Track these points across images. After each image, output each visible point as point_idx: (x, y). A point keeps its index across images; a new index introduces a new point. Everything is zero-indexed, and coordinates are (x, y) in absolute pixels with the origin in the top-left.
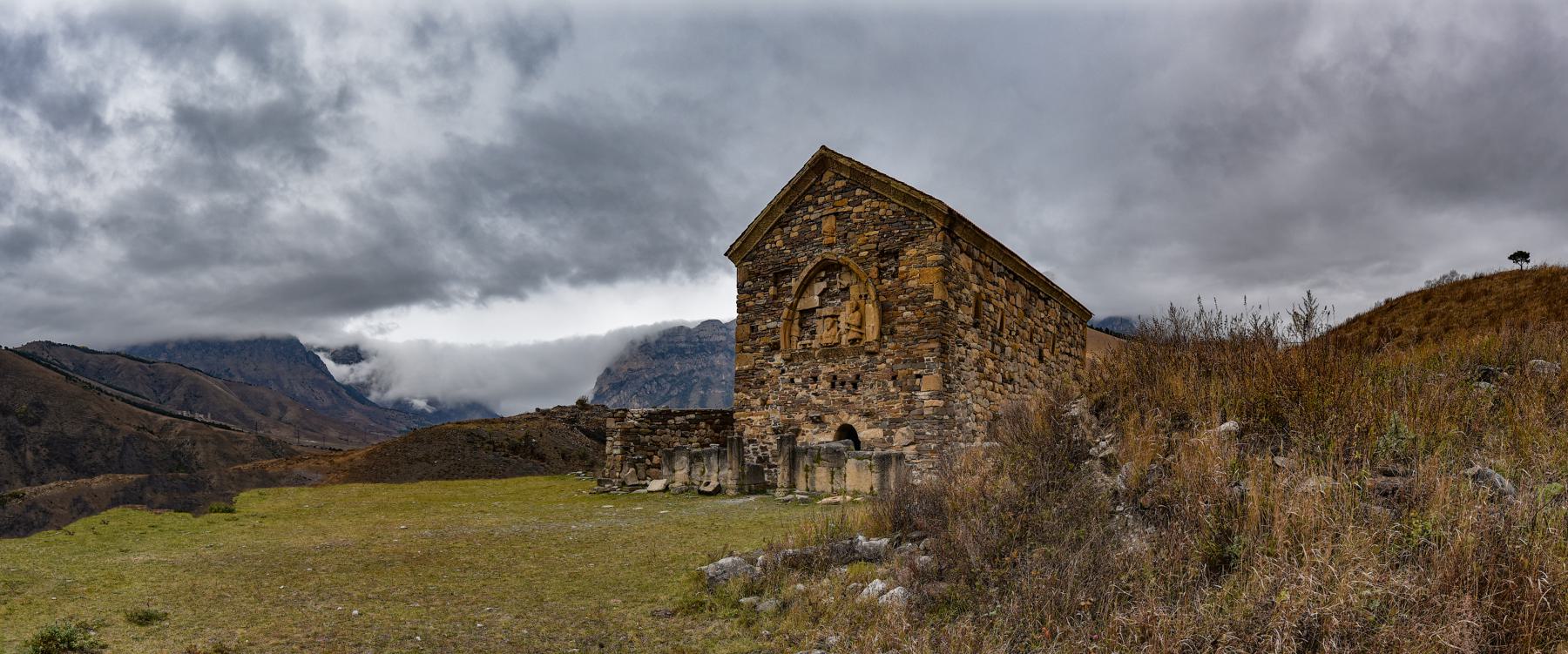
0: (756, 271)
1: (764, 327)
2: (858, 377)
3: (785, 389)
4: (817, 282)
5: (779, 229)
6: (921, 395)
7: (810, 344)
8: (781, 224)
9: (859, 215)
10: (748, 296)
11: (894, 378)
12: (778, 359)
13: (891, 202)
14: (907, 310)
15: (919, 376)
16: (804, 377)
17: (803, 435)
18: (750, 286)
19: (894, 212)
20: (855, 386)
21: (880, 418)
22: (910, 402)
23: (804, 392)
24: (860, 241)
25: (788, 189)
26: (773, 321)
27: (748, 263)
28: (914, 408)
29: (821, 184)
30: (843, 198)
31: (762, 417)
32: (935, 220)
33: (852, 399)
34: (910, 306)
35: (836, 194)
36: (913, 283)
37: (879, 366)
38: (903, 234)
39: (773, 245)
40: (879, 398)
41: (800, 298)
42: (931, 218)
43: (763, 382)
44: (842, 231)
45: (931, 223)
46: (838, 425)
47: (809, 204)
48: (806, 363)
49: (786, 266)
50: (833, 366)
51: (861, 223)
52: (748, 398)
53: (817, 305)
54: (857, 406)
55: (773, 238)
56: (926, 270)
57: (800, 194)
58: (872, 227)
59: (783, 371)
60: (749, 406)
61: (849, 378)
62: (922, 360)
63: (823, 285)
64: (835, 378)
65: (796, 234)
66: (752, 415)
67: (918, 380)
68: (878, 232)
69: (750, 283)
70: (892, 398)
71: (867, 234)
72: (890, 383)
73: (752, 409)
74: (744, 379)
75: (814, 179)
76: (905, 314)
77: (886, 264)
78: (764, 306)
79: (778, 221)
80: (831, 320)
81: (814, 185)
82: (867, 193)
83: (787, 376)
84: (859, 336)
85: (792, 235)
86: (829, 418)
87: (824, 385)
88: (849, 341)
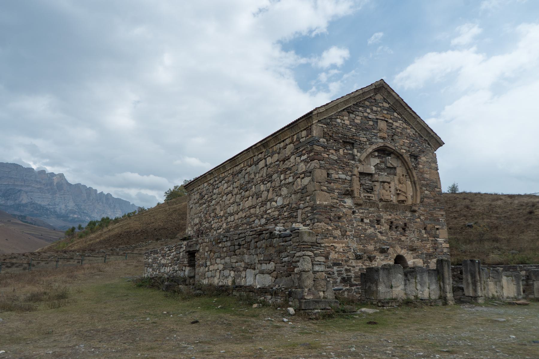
0: (330, 134)
1: (337, 176)
2: (405, 224)
3: (359, 226)
4: (372, 157)
5: (347, 113)
6: (440, 240)
7: (372, 197)
8: (349, 111)
10: (323, 149)
11: (425, 229)
12: (349, 202)
13: (412, 128)
14: (427, 190)
15: (437, 229)
16: (371, 219)
17: (375, 261)
18: (324, 142)
19: (413, 134)
21: (420, 252)
22: (435, 244)
23: (372, 230)
24: (401, 143)
25: (361, 92)
26: (343, 174)
27: (324, 126)
28: (438, 248)
29: (375, 99)
30: (387, 114)
31: (344, 245)
32: (433, 146)
33: (403, 238)
35: (384, 109)
38: (419, 148)
39: (343, 122)
40: (418, 239)
42: (431, 144)
43: (339, 218)
45: (430, 147)
46: (395, 255)
47: (368, 107)
50: (390, 215)
52: (330, 228)
53: (374, 172)
54: (406, 243)
55: (343, 116)
57: (364, 99)
58: (406, 138)
59: (354, 212)
60: (331, 235)
61: (401, 225)
62: (438, 220)
63: (377, 161)
64: (392, 222)
66: (335, 243)
67: (438, 231)
68: (408, 141)
70: (425, 241)
71: (404, 140)
72: (423, 231)
73: (335, 238)
74: (325, 213)
75: (372, 95)
76: (426, 192)
81: (370, 97)
82: (400, 117)
83: (358, 216)
85: (356, 121)
86: (391, 250)
87: (385, 227)
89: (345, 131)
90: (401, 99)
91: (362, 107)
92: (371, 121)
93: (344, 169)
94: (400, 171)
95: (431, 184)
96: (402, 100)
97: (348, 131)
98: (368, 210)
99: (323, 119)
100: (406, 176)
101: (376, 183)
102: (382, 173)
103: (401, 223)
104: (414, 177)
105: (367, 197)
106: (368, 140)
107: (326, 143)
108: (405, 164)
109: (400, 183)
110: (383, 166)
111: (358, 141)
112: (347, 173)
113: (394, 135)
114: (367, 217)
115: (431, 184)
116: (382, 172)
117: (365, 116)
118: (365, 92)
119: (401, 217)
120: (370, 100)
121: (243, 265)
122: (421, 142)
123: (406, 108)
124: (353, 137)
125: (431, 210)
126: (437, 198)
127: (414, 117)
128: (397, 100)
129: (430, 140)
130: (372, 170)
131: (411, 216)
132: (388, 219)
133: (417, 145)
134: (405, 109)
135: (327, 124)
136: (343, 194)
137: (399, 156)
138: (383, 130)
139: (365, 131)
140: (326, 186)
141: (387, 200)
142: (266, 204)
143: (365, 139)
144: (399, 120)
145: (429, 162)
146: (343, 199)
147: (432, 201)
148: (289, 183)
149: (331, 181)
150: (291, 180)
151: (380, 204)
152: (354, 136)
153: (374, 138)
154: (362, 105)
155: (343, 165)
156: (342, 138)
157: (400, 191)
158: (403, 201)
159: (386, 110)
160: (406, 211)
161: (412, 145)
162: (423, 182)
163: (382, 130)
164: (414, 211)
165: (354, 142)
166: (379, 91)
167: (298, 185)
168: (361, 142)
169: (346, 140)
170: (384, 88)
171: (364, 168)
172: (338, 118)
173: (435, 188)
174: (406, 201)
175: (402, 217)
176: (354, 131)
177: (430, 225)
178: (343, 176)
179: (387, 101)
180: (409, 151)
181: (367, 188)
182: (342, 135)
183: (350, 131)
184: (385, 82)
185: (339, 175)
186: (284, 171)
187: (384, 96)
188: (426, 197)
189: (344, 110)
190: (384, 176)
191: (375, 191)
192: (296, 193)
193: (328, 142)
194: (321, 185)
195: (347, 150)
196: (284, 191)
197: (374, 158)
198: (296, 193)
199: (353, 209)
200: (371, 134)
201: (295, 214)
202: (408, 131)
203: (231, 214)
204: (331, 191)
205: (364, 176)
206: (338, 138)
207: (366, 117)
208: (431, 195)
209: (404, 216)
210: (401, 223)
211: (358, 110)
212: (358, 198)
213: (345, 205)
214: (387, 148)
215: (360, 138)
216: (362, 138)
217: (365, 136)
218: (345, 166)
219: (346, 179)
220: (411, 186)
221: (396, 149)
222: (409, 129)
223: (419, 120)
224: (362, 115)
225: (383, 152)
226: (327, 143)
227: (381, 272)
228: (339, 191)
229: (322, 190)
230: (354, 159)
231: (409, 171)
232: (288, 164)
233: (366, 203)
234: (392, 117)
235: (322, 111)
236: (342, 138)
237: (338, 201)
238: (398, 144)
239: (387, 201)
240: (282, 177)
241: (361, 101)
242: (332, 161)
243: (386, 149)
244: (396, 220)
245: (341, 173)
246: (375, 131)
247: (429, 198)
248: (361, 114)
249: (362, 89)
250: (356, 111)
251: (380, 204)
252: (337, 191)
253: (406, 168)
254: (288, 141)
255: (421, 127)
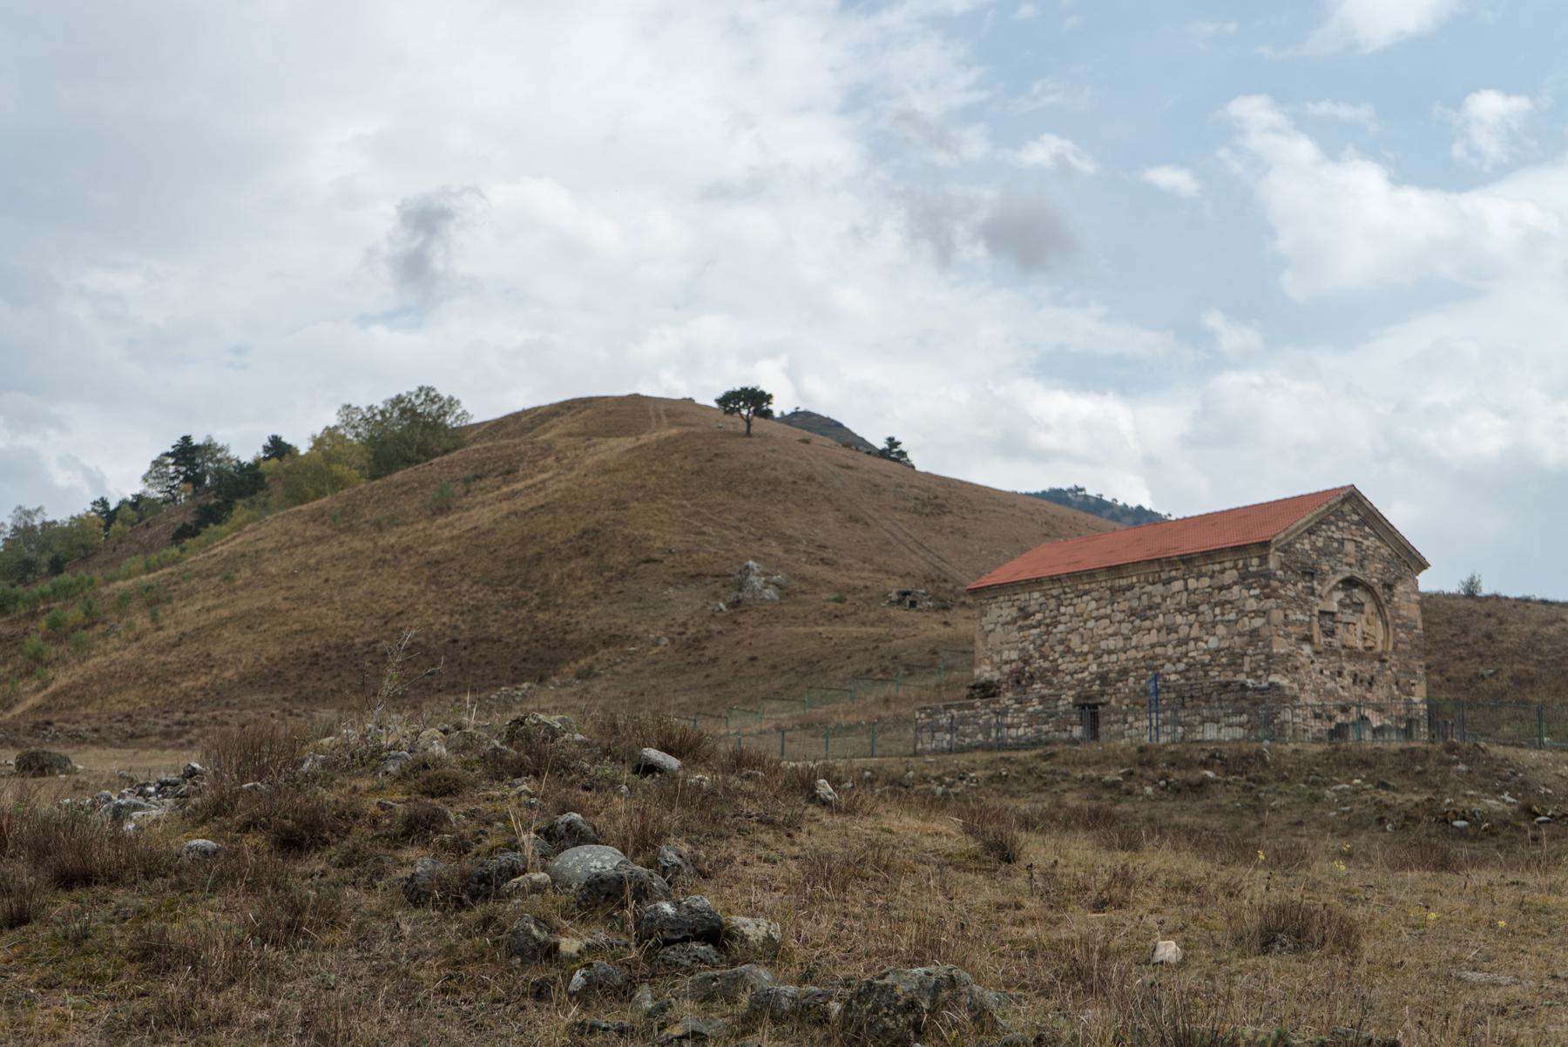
2: (1372, 678)
8: (1311, 532)
9: (1368, 547)
11: (1397, 684)
20: (1370, 684)
24: (1372, 569)
47: (1332, 523)
48: (1333, 658)
59: (1312, 662)
64: (1356, 675)
72: (1394, 687)
83: (1317, 666)
87: (1348, 681)
94: (1369, 607)
106: (1332, 568)
109: (1368, 623)
110: (1348, 601)
121: (1198, 718)
130: (1335, 607)
135: (1285, 551)
137: (1368, 589)
142: (1187, 644)
143: (1327, 568)
147: (1409, 647)
148: (1229, 621)
150: (1232, 616)
151: (1343, 652)
158: (1371, 648)
164: (1384, 661)
167: (1244, 626)
178: (1301, 617)
186: (1222, 604)
190: (1347, 616)
192: (1240, 634)
196: (1221, 630)
198: (1240, 634)
201: (1239, 661)
202: (1383, 551)
203: (1110, 652)
204: (1287, 636)
207: (1330, 537)
225: (1350, 583)
227: (1351, 727)
230: (1313, 594)
232: (1225, 595)
239: (1351, 648)
240: (1218, 611)
247: (1404, 643)
248: (1324, 534)
251: (1343, 652)
254: (1227, 565)
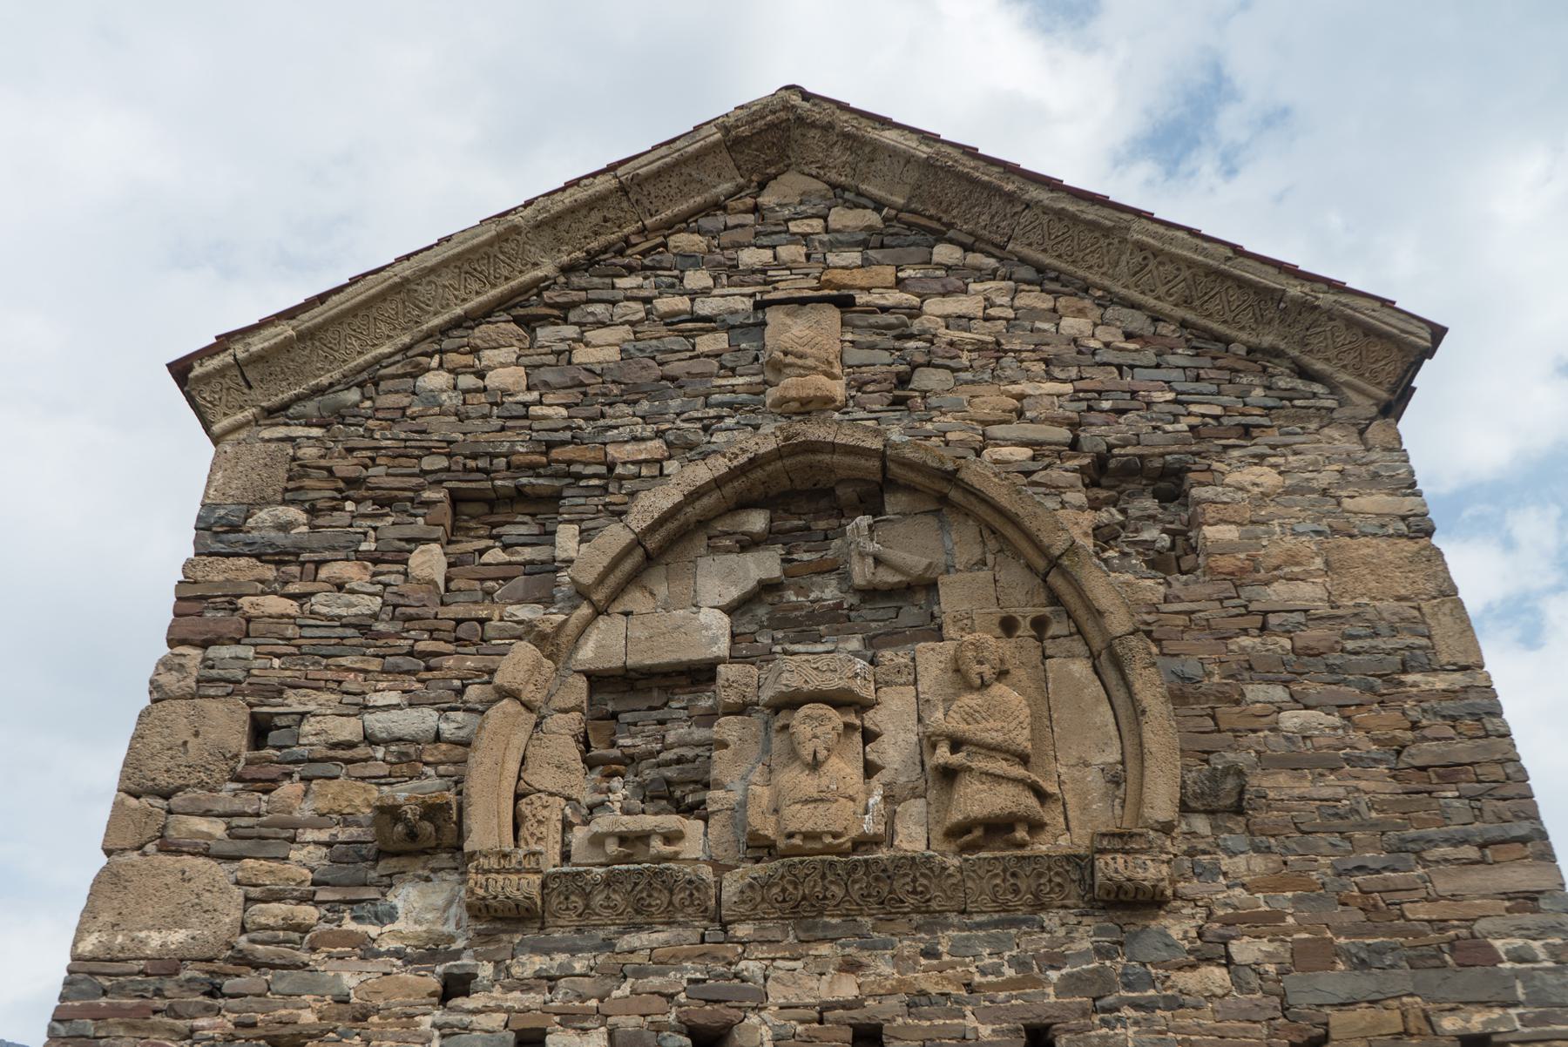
0: (345, 467)
1: (348, 729)
4: (713, 550)
7: (671, 837)
10: (270, 572)
13: (1109, 300)
16: (629, 1023)
18: (285, 527)
25: (604, 184)
29: (756, 209)
30: (866, 263)
32: (1343, 377)
34: (1313, 689)
35: (833, 246)
36: (1309, 593)
37: (1187, 980)
38: (1194, 408)
39: (467, 381)
41: (599, 612)
42: (1319, 366)
44: (881, 362)
45: (1317, 388)
47: (690, 260)
49: (532, 468)
50: (851, 967)
51: (980, 347)
55: (475, 351)
56: (1362, 548)
59: (455, 987)
62: (1474, 953)
63: (764, 565)
65: (613, 354)
68: (1068, 388)
69: (294, 513)
71: (1015, 389)
75: (726, 187)
76: (1291, 720)
77: (1110, 515)
78: (363, 627)
79: (514, 293)
80: (837, 718)
81: (717, 206)
82: (992, 262)
84: (1032, 801)
85: (581, 355)
88: (955, 832)
89: (482, 433)
90: (956, 153)
91: (645, 268)
92: (714, 330)
93: (428, 669)
95: (1350, 645)
96: (971, 152)
97: (503, 429)
98: (608, 944)
99: (298, 399)
100: (1040, 625)
101: (728, 728)
102: (820, 648)
103: (985, 1031)
104: (1100, 613)
105: (612, 847)
107: (305, 529)
108: (1010, 532)
110: (829, 592)
111: (589, 470)
112: (460, 692)
113: (915, 367)
114: (586, 1016)
115: (1350, 645)
116: (818, 639)
117: (662, 317)
118: (639, 181)
119: (983, 973)
120: (705, 223)
122: (1213, 374)
123: (1010, 187)
124: (546, 454)
125: (1360, 868)
126: (1425, 753)
127: (1093, 225)
128: (928, 164)
129: (1304, 344)
131: (1101, 952)
132: (827, 1007)
133: (1170, 396)
134: (1010, 198)
136: (381, 854)
138: (801, 357)
139: (651, 398)
140: (219, 808)
141: (809, 836)
143: (655, 448)
144: (980, 280)
145: (1313, 490)
146: (371, 893)
147: (1377, 784)
149: (274, 771)
152: (550, 445)
153: (729, 422)
154: (647, 262)
155: (425, 645)
156: (444, 476)
157: (956, 744)
158: (998, 828)
159: (864, 245)
160: (1041, 906)
161: (1106, 405)
162: (1245, 641)
163: (790, 359)
164: (1149, 901)
165: (557, 483)
166: (783, 155)
168: (619, 470)
169: (488, 484)
170: (813, 125)
171: (638, 632)
172: (428, 370)
173: (1405, 671)
174: (1036, 826)
175: (997, 971)
176: (564, 412)
177: (1362, 1015)
178: (420, 720)
179: (859, 194)
180: (1074, 445)
181: (669, 782)
182: (449, 456)
183: (526, 423)
184: (806, 96)
185: (369, 718)
187: (833, 176)
188: (1294, 765)
189: (484, 315)
191: (720, 786)
193: (319, 522)
194: (170, 812)
195: (505, 547)
197: (728, 551)
199: (457, 955)
200: (707, 405)
202: (1070, 325)
205: (656, 698)
206: (415, 481)
207: (670, 319)
208: (1356, 736)
209: (1019, 963)
210: (985, 1031)
211: (620, 295)
212: (493, 863)
213: (373, 930)
214: (826, 458)
215: (610, 449)
216: (628, 447)
217: (649, 430)
218: (451, 648)
219: (438, 737)
220: (1095, 688)
221: (895, 446)
222: (1081, 312)
223: (1147, 232)
224: (642, 314)
226: (313, 528)
228: (343, 835)
229: (169, 847)
231: (1055, 580)
233: (587, 896)
234: (900, 275)
235: (266, 344)
236: (444, 476)
237: (308, 913)
238: (949, 418)
241: (626, 239)
242: (318, 632)
243: (830, 469)
244: (917, 1001)
245: (394, 698)
246: (740, 380)
249: (612, 168)
250: (589, 301)
252: (324, 836)
253: (1030, 567)
255: (1186, 273)
